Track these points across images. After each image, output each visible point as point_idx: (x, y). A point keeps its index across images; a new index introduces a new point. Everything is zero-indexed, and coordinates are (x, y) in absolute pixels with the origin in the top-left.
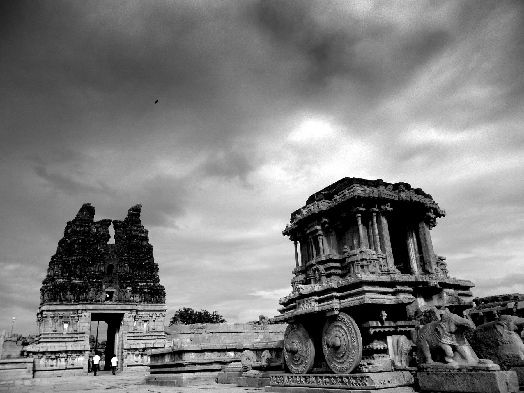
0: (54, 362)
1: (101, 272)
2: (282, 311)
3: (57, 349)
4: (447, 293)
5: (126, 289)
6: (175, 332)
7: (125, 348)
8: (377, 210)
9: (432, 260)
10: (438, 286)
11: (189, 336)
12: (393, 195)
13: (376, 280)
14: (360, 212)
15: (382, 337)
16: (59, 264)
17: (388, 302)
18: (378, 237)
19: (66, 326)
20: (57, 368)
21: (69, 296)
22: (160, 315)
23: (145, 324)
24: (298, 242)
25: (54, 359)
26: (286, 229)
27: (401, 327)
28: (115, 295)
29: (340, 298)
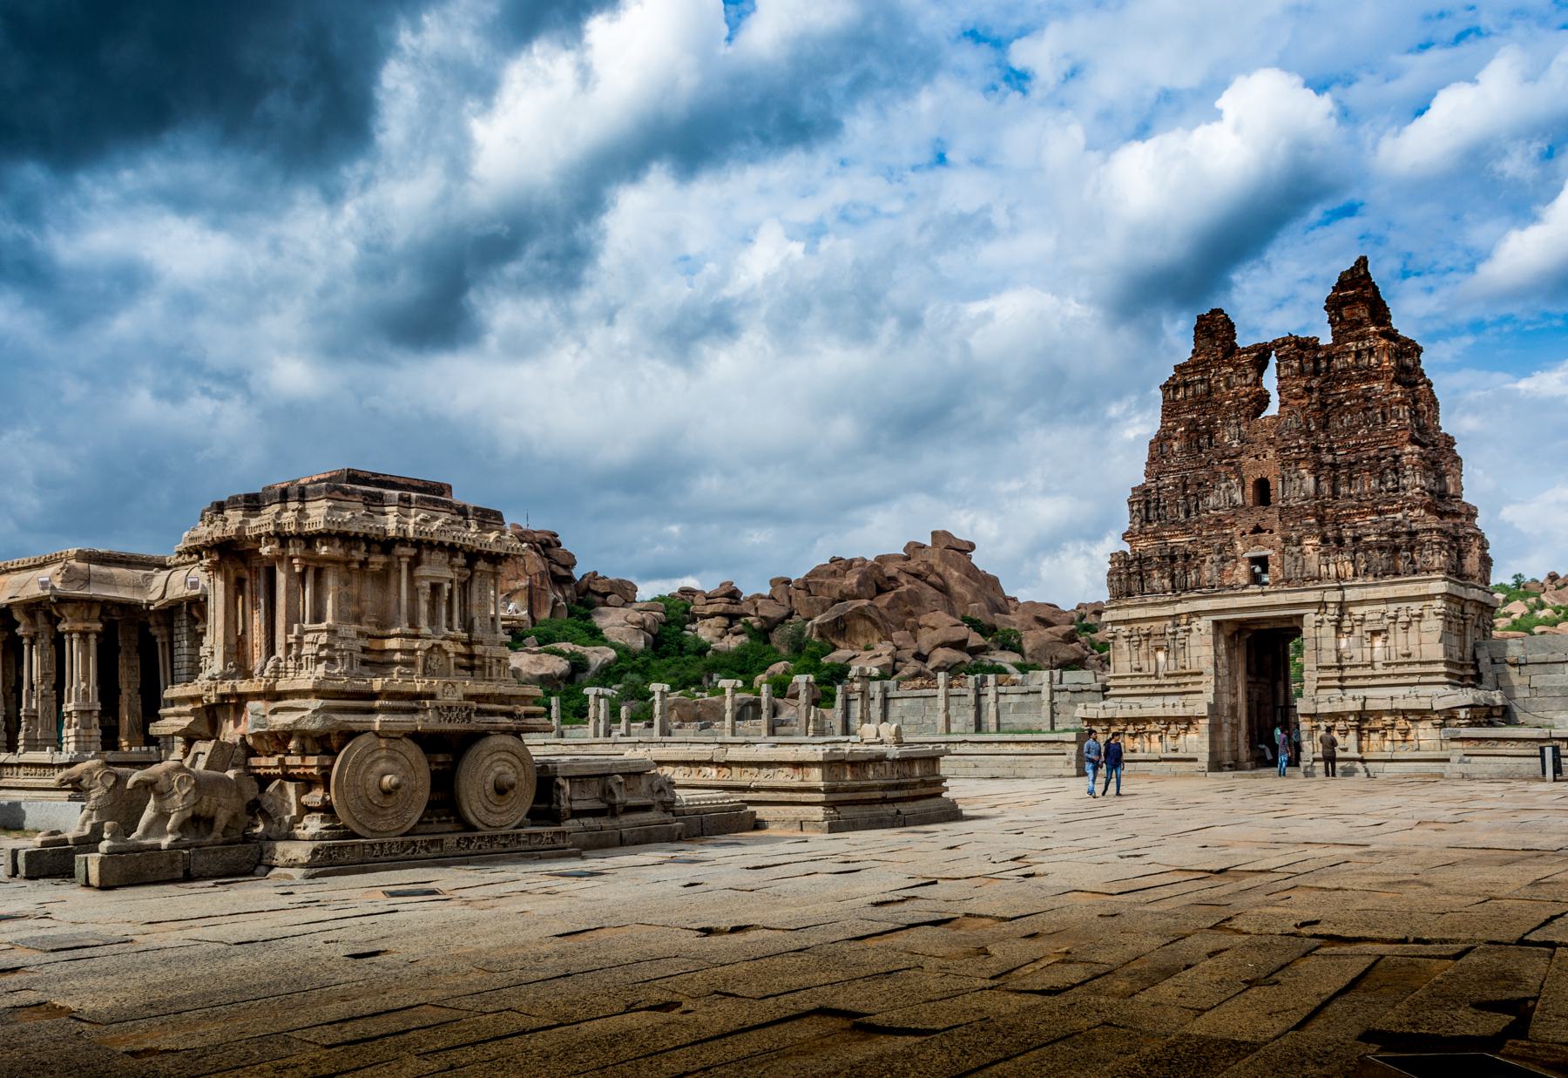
3: (1136, 713)
19: (1161, 656)
21: (1158, 580)
22: (1426, 612)
23: (1378, 642)
28: (1271, 566)
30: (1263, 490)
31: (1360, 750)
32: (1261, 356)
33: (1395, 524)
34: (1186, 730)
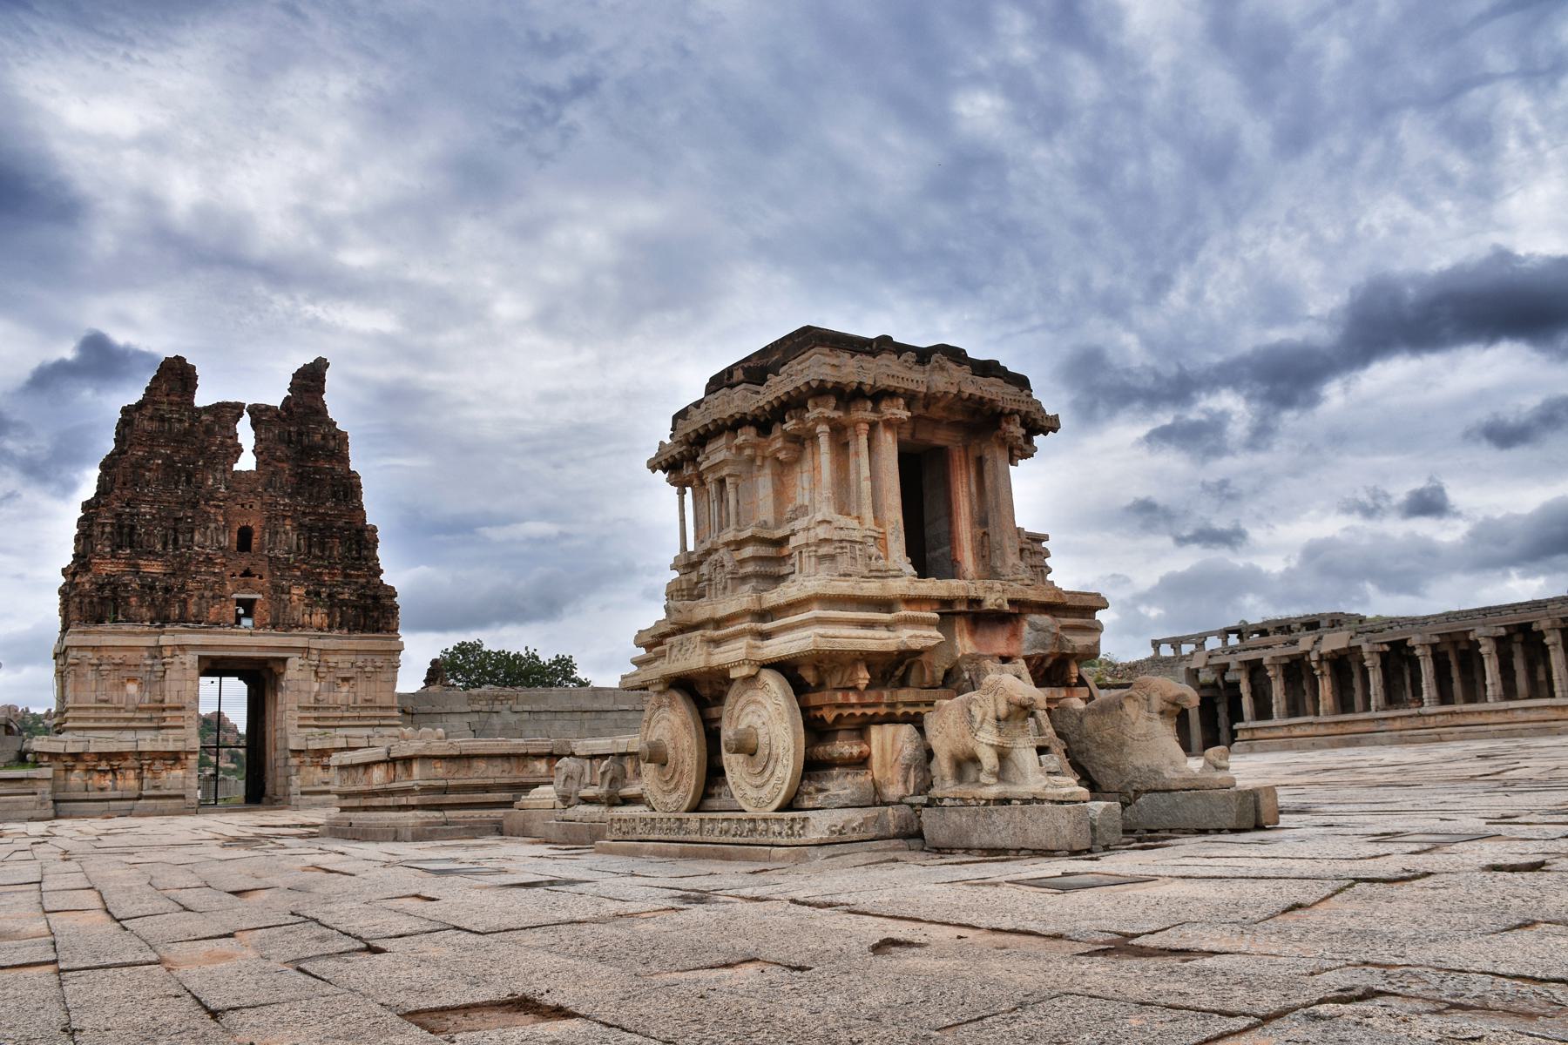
0: (107, 781)
1: (221, 549)
2: (639, 663)
3: (113, 748)
4: (1031, 625)
6: (427, 708)
7: (293, 747)
8: (872, 416)
9: (1007, 543)
10: (1007, 607)
11: (466, 719)
12: (917, 379)
13: (849, 591)
14: (828, 421)
15: (861, 729)
16: (104, 525)
17: (873, 646)
18: (866, 486)
19: (132, 688)
20: (117, 794)
23: (345, 688)
24: (689, 489)
25: (105, 772)
26: (657, 455)
27: (906, 704)
28: (258, 608)
29: (765, 636)
30: (245, 536)
33: (363, 587)
34: (172, 767)
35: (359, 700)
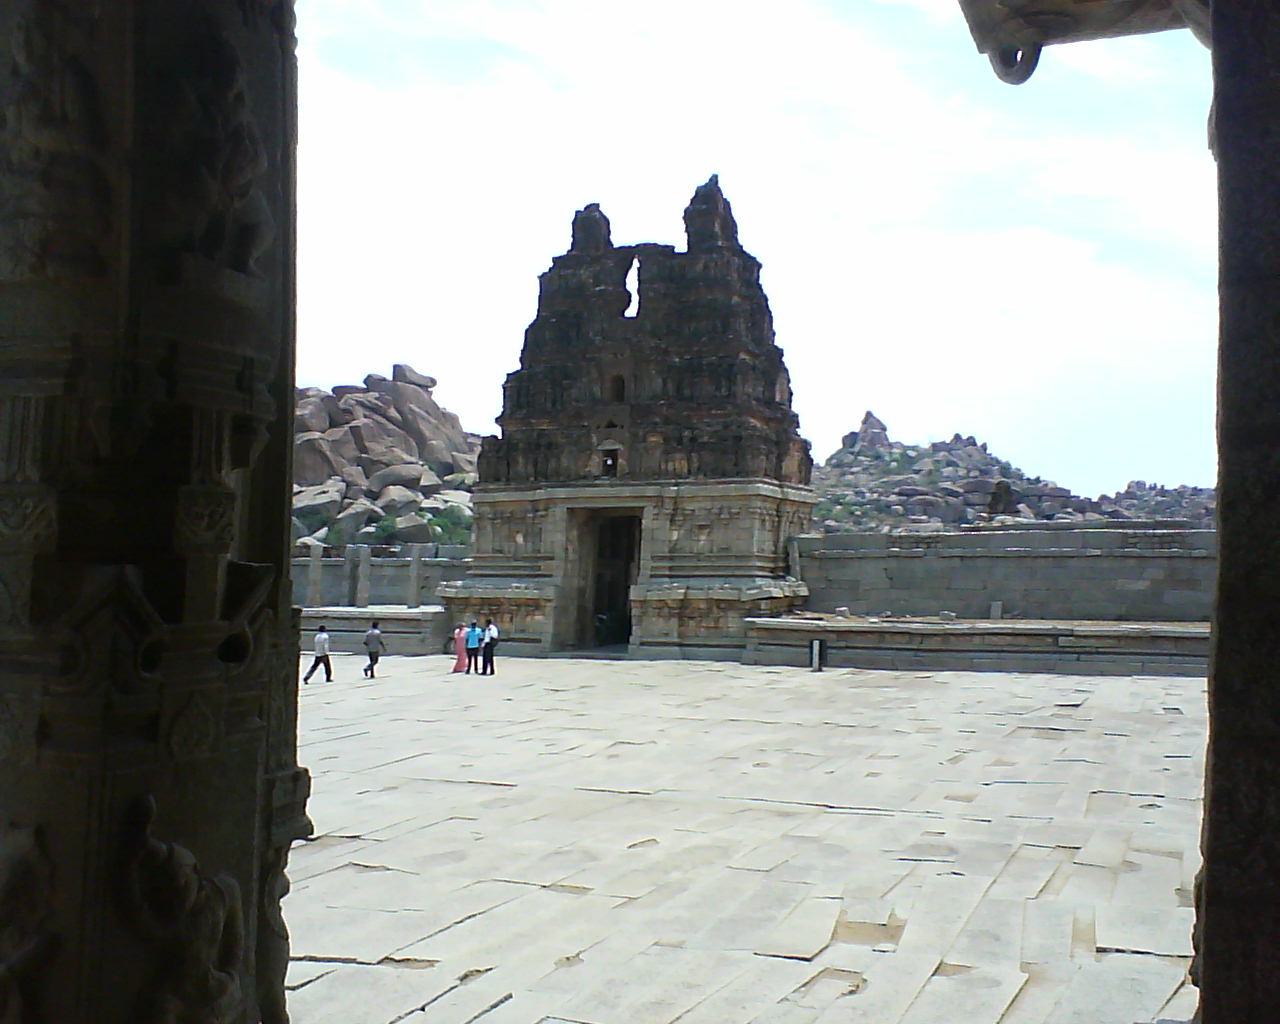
5: (644, 441)
11: (883, 564)
19: (520, 539)
23: (703, 537)
28: (620, 461)
31: (680, 636)
32: (628, 253)
35: (715, 549)
